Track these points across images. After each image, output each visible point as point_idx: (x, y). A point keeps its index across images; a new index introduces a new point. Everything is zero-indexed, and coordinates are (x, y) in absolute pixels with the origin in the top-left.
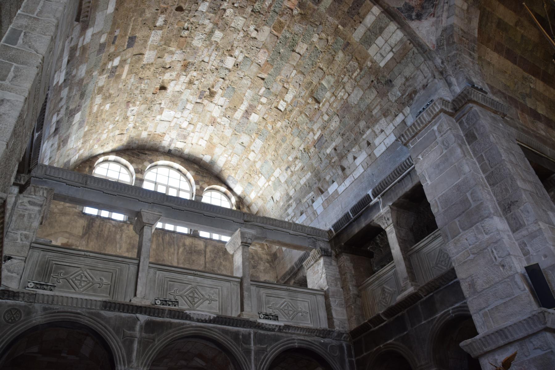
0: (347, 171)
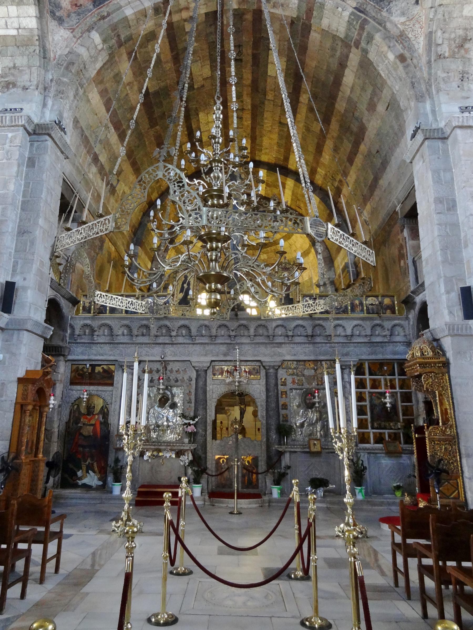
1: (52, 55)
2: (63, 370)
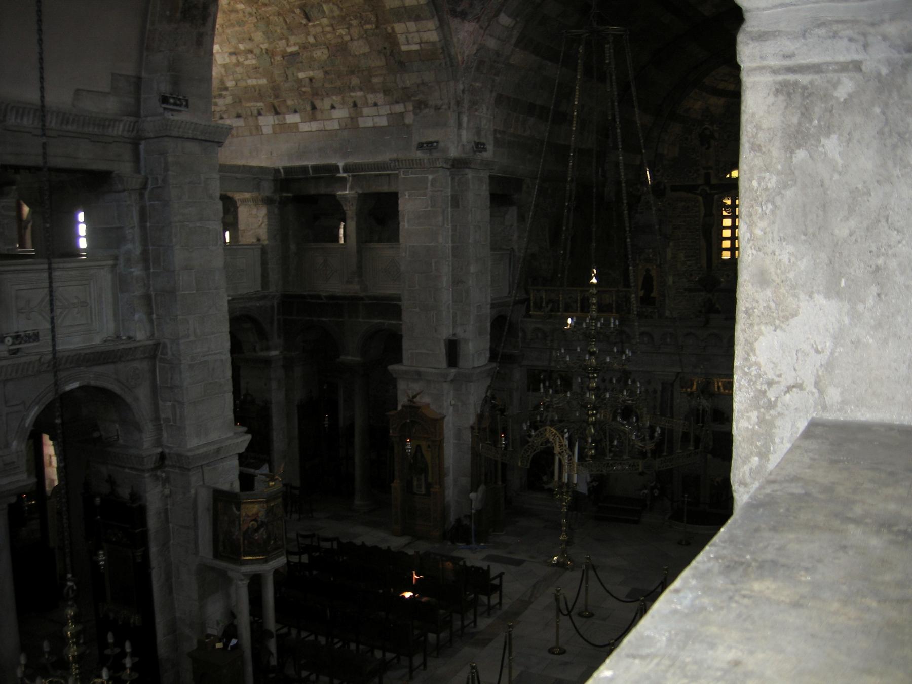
0: (318, 115)
1: (460, 58)
2: (518, 376)
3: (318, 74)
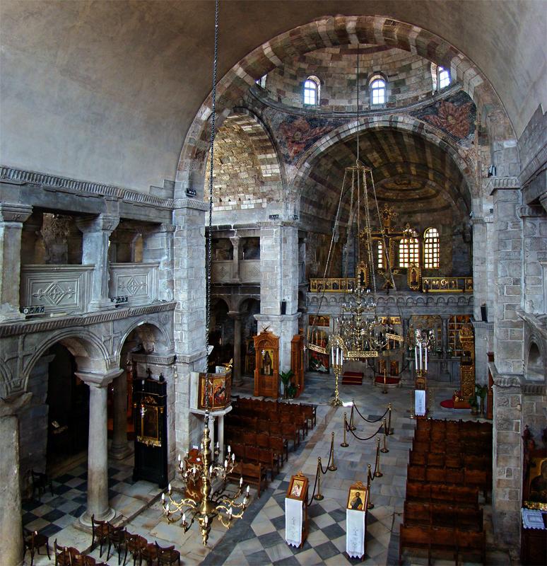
0: (223, 203)
3: (224, 186)
